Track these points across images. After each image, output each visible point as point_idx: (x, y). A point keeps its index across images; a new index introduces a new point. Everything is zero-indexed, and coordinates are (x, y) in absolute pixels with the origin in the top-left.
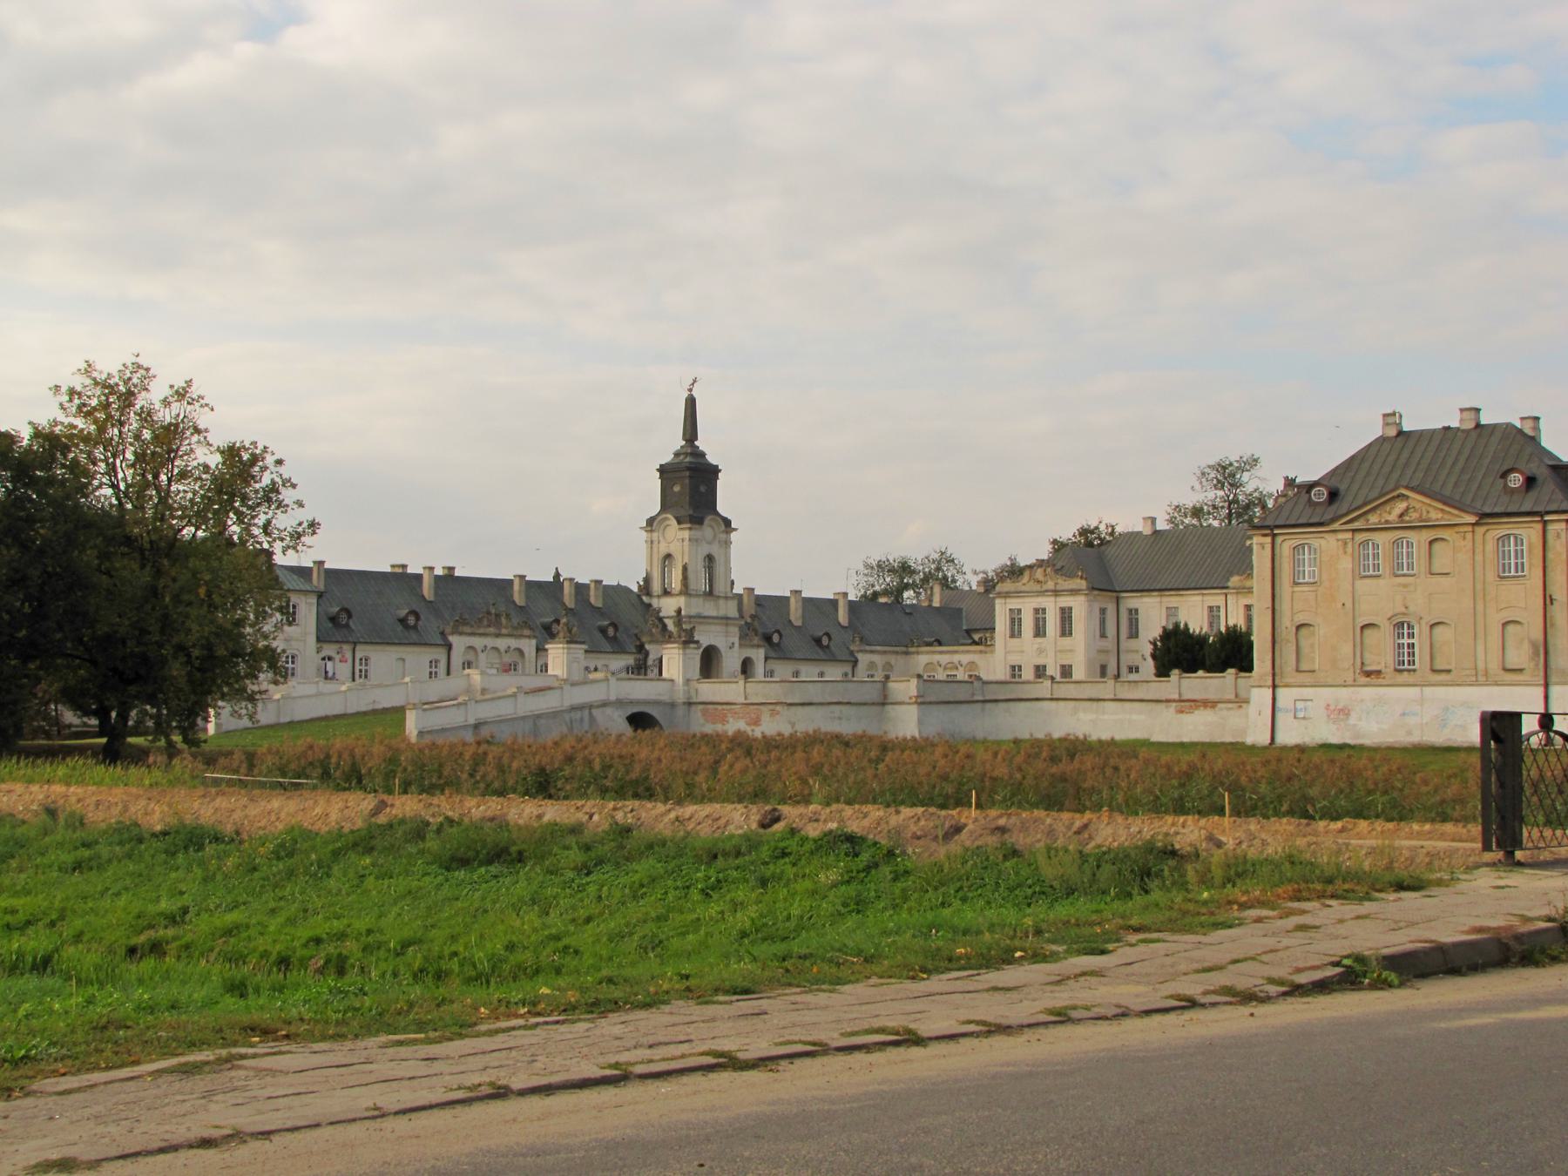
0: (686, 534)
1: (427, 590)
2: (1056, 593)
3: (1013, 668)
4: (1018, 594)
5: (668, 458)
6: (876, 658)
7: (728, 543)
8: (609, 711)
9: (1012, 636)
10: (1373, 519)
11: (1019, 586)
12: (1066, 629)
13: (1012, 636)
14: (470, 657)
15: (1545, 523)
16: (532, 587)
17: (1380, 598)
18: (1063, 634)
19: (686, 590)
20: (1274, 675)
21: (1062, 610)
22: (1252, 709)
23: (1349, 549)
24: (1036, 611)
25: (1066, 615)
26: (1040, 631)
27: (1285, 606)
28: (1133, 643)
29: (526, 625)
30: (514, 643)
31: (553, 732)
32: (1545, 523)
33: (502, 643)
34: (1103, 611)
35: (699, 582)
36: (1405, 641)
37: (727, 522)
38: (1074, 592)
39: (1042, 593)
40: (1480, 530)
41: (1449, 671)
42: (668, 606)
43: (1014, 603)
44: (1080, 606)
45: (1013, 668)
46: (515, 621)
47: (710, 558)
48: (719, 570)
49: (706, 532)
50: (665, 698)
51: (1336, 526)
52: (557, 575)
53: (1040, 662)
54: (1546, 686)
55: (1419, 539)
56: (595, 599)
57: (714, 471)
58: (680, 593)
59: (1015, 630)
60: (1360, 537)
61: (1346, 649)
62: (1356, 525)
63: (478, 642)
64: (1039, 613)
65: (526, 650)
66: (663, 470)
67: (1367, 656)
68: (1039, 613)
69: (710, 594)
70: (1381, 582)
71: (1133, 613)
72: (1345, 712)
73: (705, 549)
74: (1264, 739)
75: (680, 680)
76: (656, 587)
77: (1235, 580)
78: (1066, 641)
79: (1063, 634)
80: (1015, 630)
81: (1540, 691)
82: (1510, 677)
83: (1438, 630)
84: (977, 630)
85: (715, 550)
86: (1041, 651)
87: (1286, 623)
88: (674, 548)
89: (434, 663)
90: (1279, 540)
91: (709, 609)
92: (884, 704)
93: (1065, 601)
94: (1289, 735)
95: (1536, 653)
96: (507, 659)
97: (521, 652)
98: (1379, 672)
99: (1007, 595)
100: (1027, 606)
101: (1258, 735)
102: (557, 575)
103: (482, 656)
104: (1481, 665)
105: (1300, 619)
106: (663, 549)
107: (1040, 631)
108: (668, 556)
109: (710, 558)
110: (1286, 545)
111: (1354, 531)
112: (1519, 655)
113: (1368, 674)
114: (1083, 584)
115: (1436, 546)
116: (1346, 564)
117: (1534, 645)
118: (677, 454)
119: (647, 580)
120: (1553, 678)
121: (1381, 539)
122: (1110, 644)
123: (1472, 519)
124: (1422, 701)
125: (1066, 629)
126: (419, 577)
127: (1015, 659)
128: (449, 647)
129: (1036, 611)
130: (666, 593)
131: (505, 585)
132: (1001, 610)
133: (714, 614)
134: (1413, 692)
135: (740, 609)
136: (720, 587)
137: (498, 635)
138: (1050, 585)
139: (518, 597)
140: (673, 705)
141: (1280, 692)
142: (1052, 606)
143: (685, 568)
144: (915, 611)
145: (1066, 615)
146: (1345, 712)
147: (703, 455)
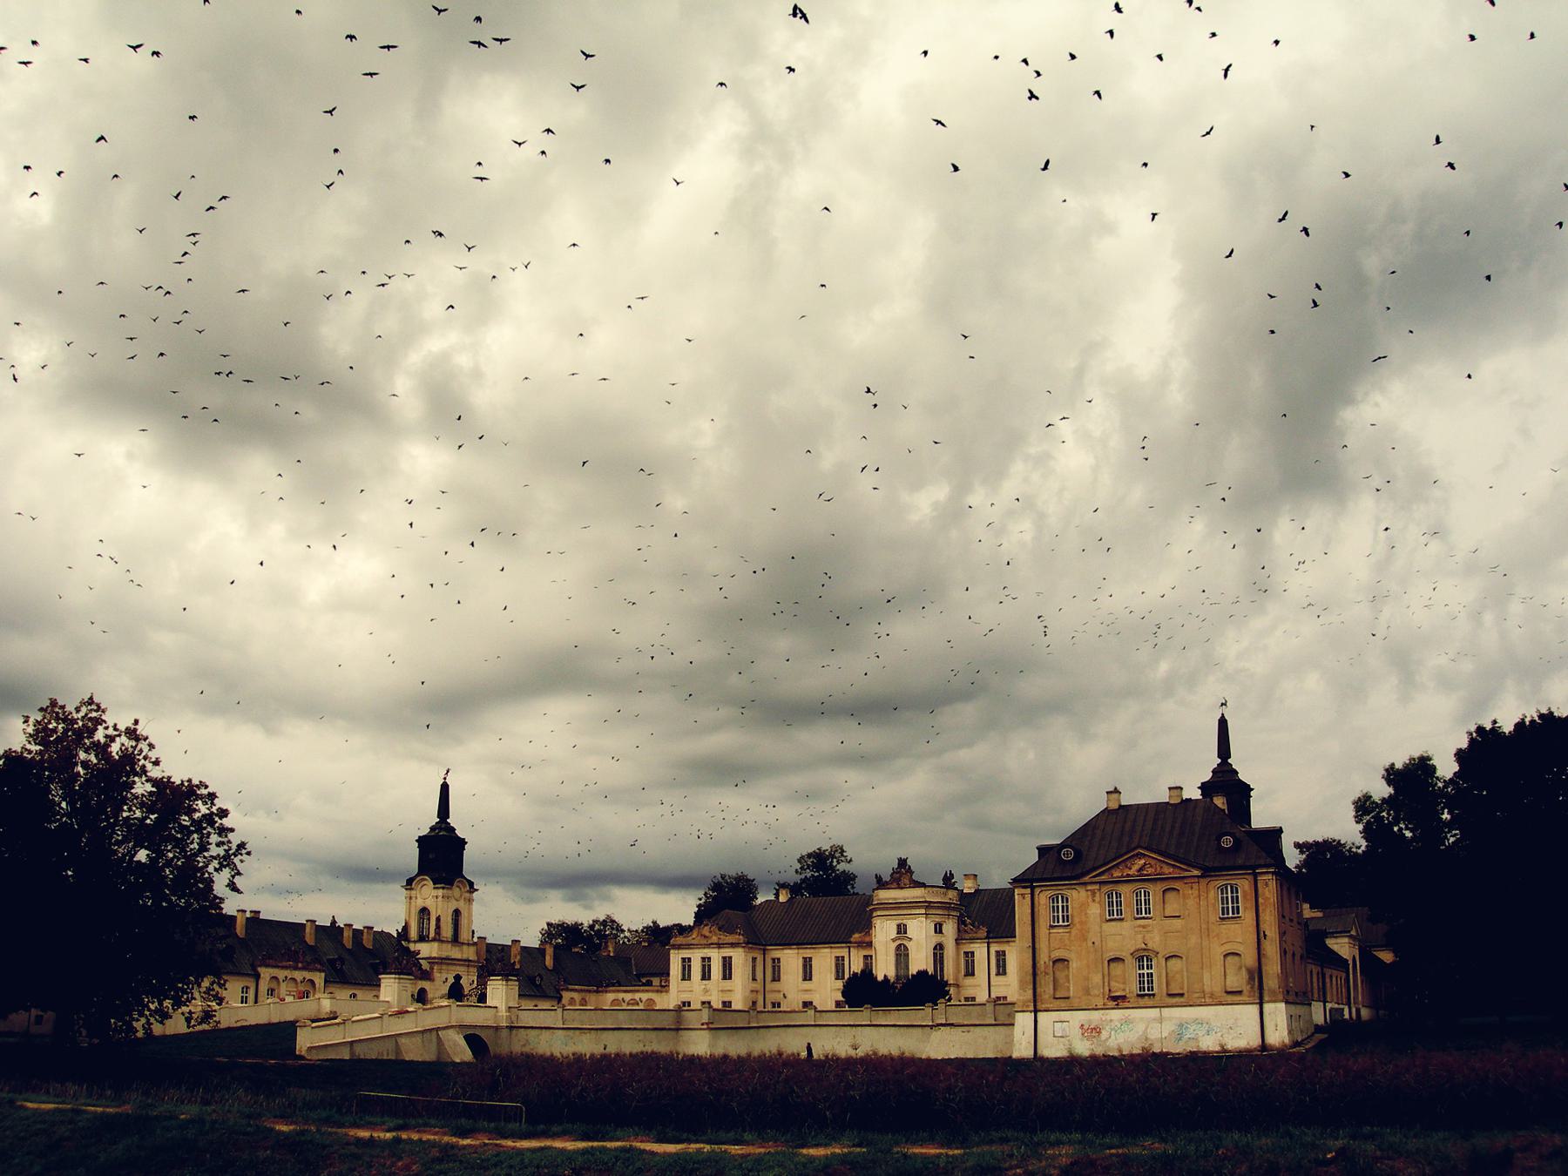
0: (440, 892)
1: (240, 929)
2: (719, 946)
4: (689, 946)
5: (425, 831)
6: (575, 995)
7: (470, 901)
8: (451, 1032)
10: (1117, 874)
11: (689, 940)
12: (727, 974)
14: (274, 985)
15: (1255, 875)
16: (320, 929)
17: (1123, 936)
18: (724, 978)
19: (438, 938)
20: (1035, 1002)
22: (1017, 1029)
23: (1097, 898)
25: (727, 964)
26: (706, 975)
27: (1042, 945)
28: (776, 985)
29: (318, 960)
30: (308, 975)
32: (1255, 875)
33: (298, 975)
34: (754, 959)
35: (447, 932)
36: (1146, 971)
37: (471, 884)
38: (733, 945)
39: (709, 946)
40: (1204, 881)
41: (1182, 995)
42: (426, 950)
43: (686, 953)
44: (739, 957)
46: (308, 958)
47: (457, 913)
48: (464, 921)
49: (456, 891)
50: (490, 1023)
51: (1086, 879)
52: (334, 922)
54: (1261, 1005)
55: (1155, 890)
56: (368, 942)
57: (463, 842)
58: (434, 940)
59: (686, 975)
60: (1105, 889)
61: (1097, 979)
62: (1103, 878)
63: (281, 974)
64: (706, 961)
65: (317, 981)
66: (421, 840)
67: (1113, 984)
68: (706, 961)
69: (455, 940)
70: (1124, 924)
71: (776, 961)
72: (1096, 1030)
73: (453, 905)
74: (1027, 1053)
75: (503, 1008)
76: (413, 934)
77: (856, 936)
79: (724, 978)
80: (686, 975)
81: (1255, 1009)
82: (1230, 998)
83: (1172, 962)
84: (644, 975)
85: (461, 905)
86: (706, 991)
87: (1043, 958)
88: (430, 904)
89: (245, 989)
90: (1037, 891)
91: (455, 953)
92: (678, 1030)
93: (727, 952)
94: (1053, 1049)
95: (1251, 978)
96: (302, 988)
97: (312, 982)
98: (1124, 997)
99: (679, 947)
100: (696, 956)
101: (1022, 1049)
102: (334, 922)
103: (283, 985)
104: (1207, 989)
105: (1057, 954)
106: (420, 903)
107: (706, 975)
108: (424, 911)
109: (457, 913)
110: (1043, 898)
111: (1100, 883)
112: (1237, 980)
113: (1115, 999)
115: (1169, 895)
116: (1095, 910)
117: (1250, 972)
118: (432, 829)
119: (406, 928)
120: (1266, 998)
121: (1125, 890)
122: (758, 986)
123: (1196, 873)
124: (1161, 1020)
125: (727, 974)
126: (233, 918)
128: (257, 977)
130: (422, 938)
131: (299, 928)
132: (675, 959)
133: (458, 956)
134: (1154, 1012)
135: (478, 953)
136: (464, 936)
137: (296, 968)
138: (714, 939)
139: (309, 937)
140: (497, 1028)
141: (1040, 1015)
142: (716, 956)
143: (438, 919)
144: (581, 959)
145: (727, 964)
146: (1096, 1030)
147: (453, 829)
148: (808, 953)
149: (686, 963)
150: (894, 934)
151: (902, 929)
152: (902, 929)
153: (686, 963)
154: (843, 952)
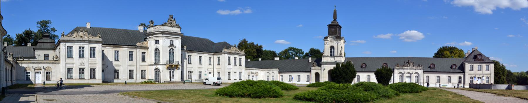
2: (90, 42)
3: (68, 69)
9: (68, 57)
12: (93, 54)
13: (68, 57)
21: (91, 48)
24: (80, 47)
26: (81, 55)
31: (297, 85)
38: (97, 42)
39: (84, 41)
45: (68, 69)
53: (82, 67)
59: (70, 55)
64: (81, 49)
68: (81, 49)
77: (138, 44)
78: (93, 60)
80: (70, 55)
86: (82, 63)
93: (93, 45)
107: (81, 55)
114: (101, 39)
125: (93, 54)
127: (70, 66)
129: (80, 47)
138: (86, 38)
142: (87, 47)
148: (117, 49)
149: (70, 49)
150: (169, 45)
151: (172, 42)
152: (172, 42)
153: (70, 49)
154: (134, 50)
